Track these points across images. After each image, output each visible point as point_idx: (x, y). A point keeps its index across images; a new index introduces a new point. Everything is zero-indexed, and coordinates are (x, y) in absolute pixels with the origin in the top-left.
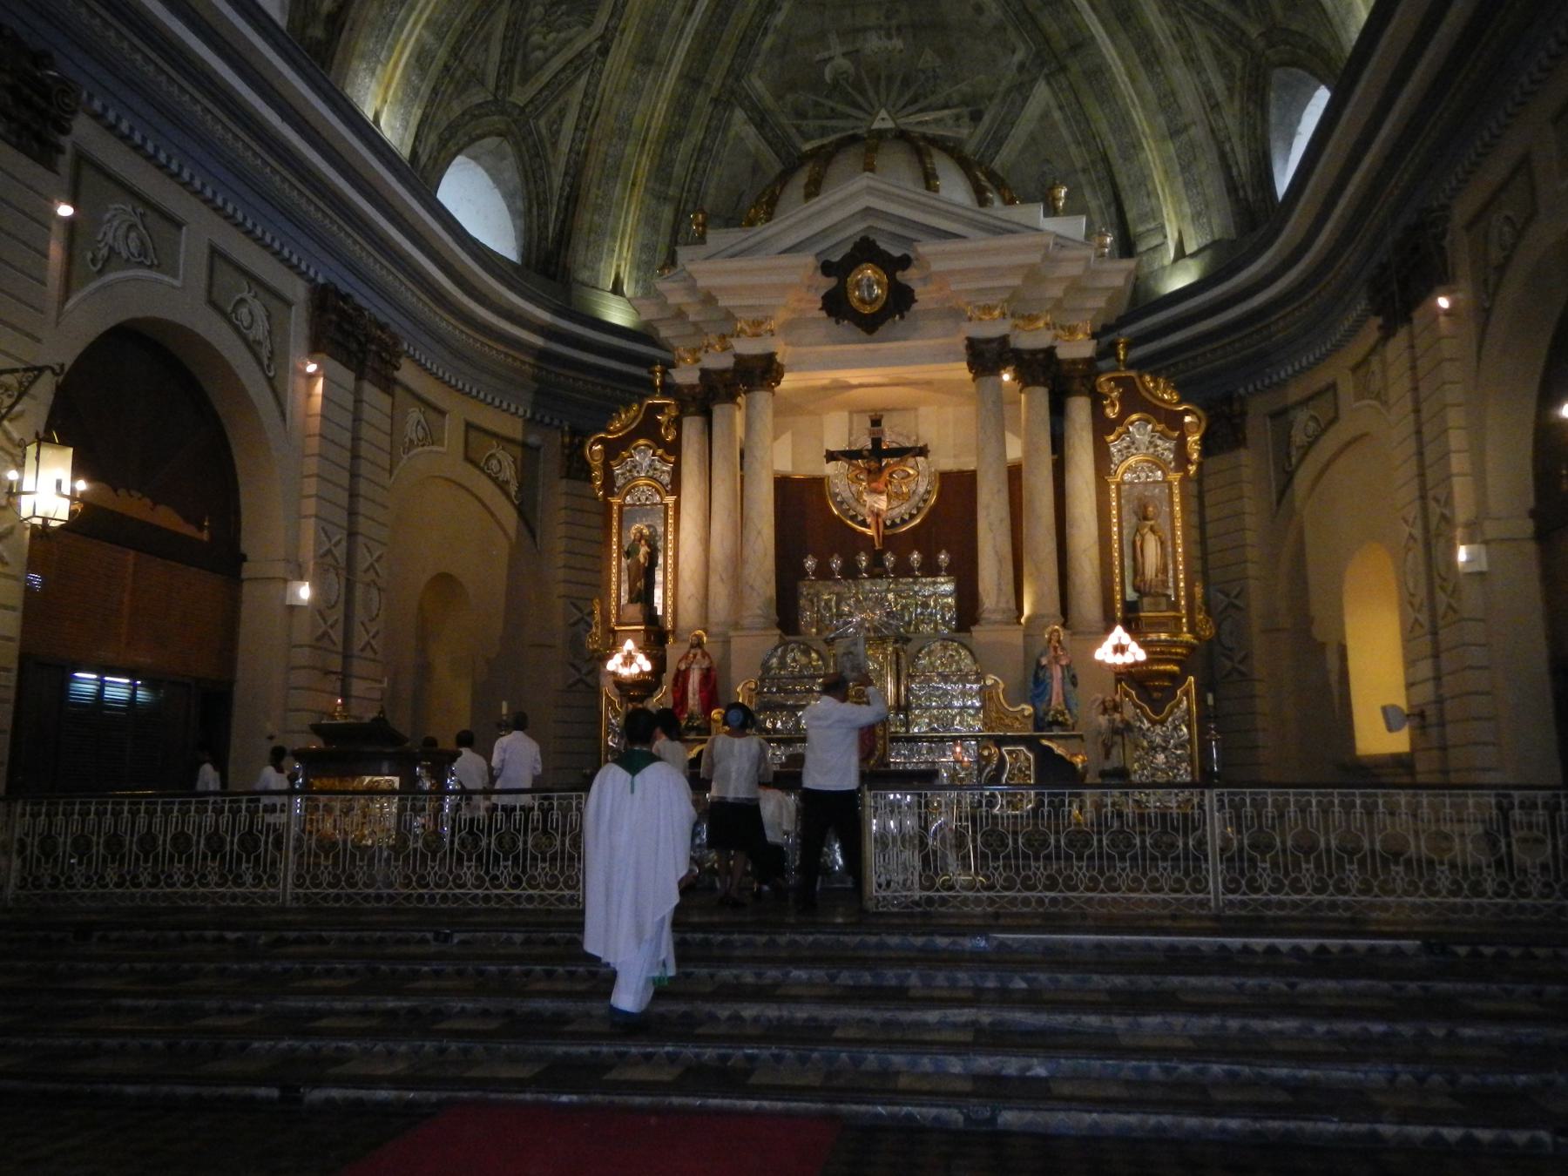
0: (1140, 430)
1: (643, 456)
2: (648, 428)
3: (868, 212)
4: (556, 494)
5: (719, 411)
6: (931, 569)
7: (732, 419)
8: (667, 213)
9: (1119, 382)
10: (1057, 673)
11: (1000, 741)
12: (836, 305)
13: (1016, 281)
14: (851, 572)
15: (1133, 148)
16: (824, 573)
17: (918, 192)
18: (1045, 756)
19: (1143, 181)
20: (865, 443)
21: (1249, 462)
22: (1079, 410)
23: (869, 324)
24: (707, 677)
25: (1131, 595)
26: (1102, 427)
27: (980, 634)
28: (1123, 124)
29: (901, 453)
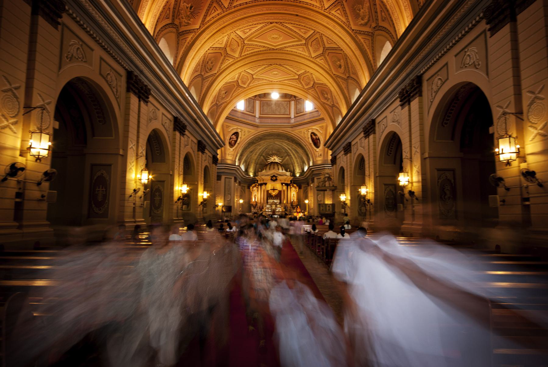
0: (293, 189)
1: (255, 188)
2: (255, 186)
4: (247, 190)
5: (262, 186)
6: (278, 199)
7: (263, 187)
8: (255, 165)
12: (272, 179)
14: (272, 199)
15: (295, 163)
16: (270, 199)
17: (278, 171)
18: (286, 213)
19: (295, 166)
20: (273, 189)
21: (302, 190)
22: (289, 187)
23: (274, 181)
27: (281, 204)
28: (294, 161)
29: (276, 189)
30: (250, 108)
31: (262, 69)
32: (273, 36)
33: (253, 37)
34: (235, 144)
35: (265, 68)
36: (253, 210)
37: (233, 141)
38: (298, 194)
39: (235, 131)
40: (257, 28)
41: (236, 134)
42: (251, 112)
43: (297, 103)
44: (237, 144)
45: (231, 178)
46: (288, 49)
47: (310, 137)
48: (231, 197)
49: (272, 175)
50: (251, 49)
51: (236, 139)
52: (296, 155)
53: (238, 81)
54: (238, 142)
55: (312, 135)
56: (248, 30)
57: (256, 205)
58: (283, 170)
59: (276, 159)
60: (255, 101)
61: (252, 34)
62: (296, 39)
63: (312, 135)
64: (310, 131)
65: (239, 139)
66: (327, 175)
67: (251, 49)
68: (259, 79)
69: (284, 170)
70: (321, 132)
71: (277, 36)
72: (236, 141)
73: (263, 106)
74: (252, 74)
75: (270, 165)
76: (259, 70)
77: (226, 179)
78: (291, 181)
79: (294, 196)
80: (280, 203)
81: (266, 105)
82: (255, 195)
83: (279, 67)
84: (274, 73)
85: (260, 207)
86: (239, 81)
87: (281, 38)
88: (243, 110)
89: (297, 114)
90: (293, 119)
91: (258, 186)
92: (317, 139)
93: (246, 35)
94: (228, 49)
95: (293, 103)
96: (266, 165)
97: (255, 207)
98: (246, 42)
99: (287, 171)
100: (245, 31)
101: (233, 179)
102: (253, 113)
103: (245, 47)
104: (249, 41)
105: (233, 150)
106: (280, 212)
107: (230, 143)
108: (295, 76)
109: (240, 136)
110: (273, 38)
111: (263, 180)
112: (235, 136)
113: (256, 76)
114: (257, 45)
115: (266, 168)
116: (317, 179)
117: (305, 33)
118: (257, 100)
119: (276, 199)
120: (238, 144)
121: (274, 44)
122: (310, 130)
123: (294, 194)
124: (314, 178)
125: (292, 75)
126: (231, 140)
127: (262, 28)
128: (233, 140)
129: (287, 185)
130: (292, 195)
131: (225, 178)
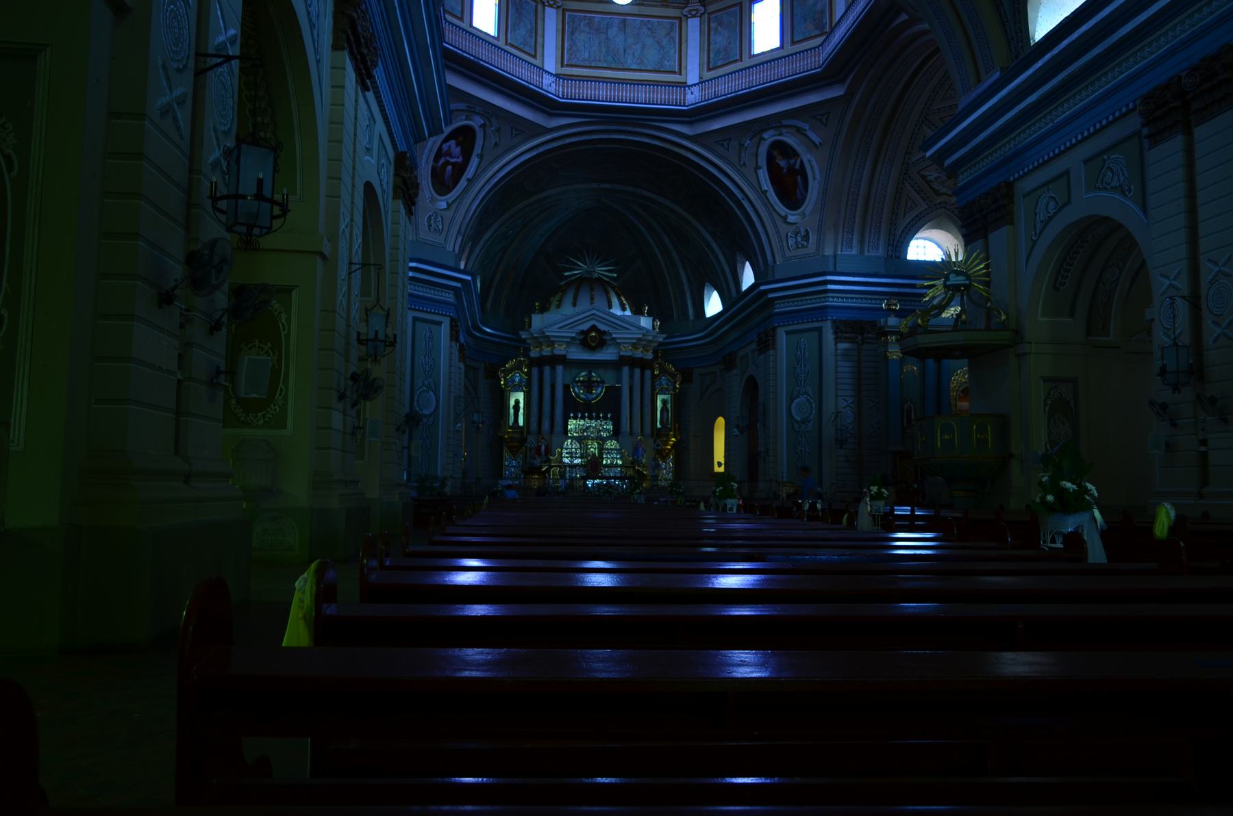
2: (518, 367)
3: (593, 314)
6: (605, 418)
9: (659, 364)
10: (641, 449)
11: (626, 467)
13: (635, 341)
14: (583, 418)
16: (575, 418)
17: (608, 310)
22: (648, 373)
23: (593, 349)
24: (547, 447)
25: (659, 426)
26: (654, 377)
29: (597, 381)
30: (522, 31)
34: (456, 183)
36: (511, 465)
37: (449, 168)
38: (679, 401)
39: (460, 122)
41: (465, 136)
42: (526, 49)
43: (713, 25)
44: (463, 183)
45: (439, 323)
47: (762, 161)
48: (437, 400)
49: (585, 327)
51: (460, 160)
52: (674, 254)
54: (470, 172)
55: (775, 153)
57: (523, 441)
58: (624, 309)
59: (601, 270)
60: (540, 7)
63: (775, 153)
64: (770, 137)
65: (474, 161)
66: (961, 280)
69: (627, 306)
70: (817, 140)
72: (460, 170)
73: (572, 33)
75: (577, 290)
77: (418, 323)
78: (655, 352)
79: (664, 409)
80: (616, 434)
81: (587, 29)
82: (517, 402)
85: (539, 447)
88: (498, 38)
89: (709, 69)
90: (695, 89)
91: (530, 367)
92: (791, 169)
95: (693, 27)
96: (564, 291)
97: (514, 452)
99: (637, 311)
101: (445, 328)
102: (535, 57)
105: (449, 205)
106: (617, 466)
107: (437, 175)
109: (477, 150)
111: (551, 344)
112: (457, 145)
115: (560, 301)
116: (788, 333)
118: (550, 6)
119: (598, 418)
120: (468, 180)
122: (765, 136)
123: (664, 402)
124: (774, 329)
126: (442, 161)
128: (448, 163)
129: (643, 364)
130: (659, 404)
131: (415, 319)
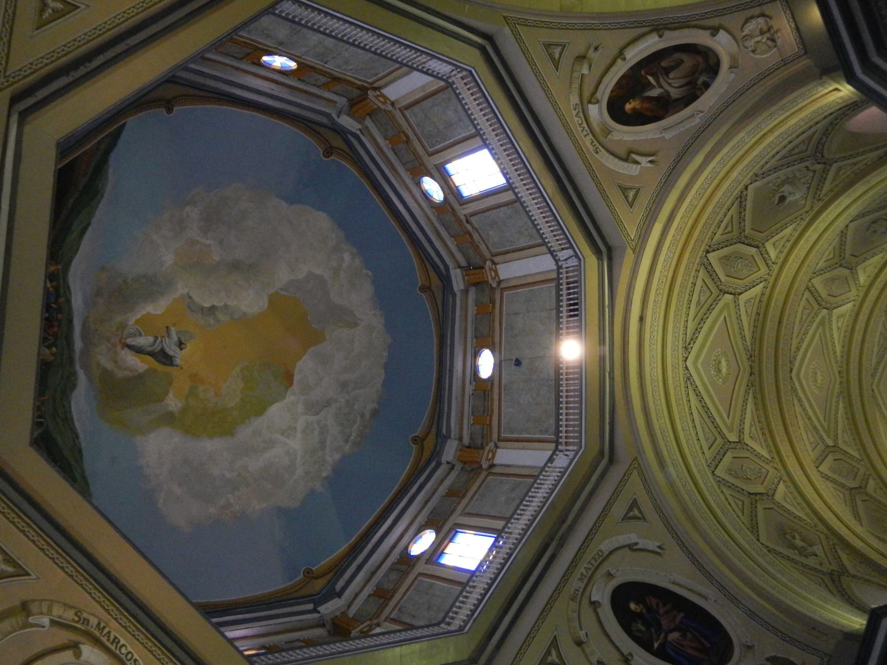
31: (741, 328)
32: (819, 374)
33: (824, 330)
35: (743, 338)
40: (836, 342)
46: (798, 409)
50: (804, 317)
53: (757, 247)
56: (840, 324)
61: (831, 329)
62: (825, 425)
67: (804, 317)
68: (710, 310)
71: (819, 382)
74: (740, 294)
76: (744, 317)
83: (745, 382)
84: (724, 363)
86: (753, 250)
87: (816, 392)
93: (834, 319)
94: (846, 272)
98: (825, 311)
100: (842, 319)
103: (816, 307)
104: (824, 317)
108: (731, 430)
110: (816, 373)
113: (726, 305)
114: (806, 334)
117: (844, 442)
121: (802, 375)
125: (729, 422)
127: (835, 352)
